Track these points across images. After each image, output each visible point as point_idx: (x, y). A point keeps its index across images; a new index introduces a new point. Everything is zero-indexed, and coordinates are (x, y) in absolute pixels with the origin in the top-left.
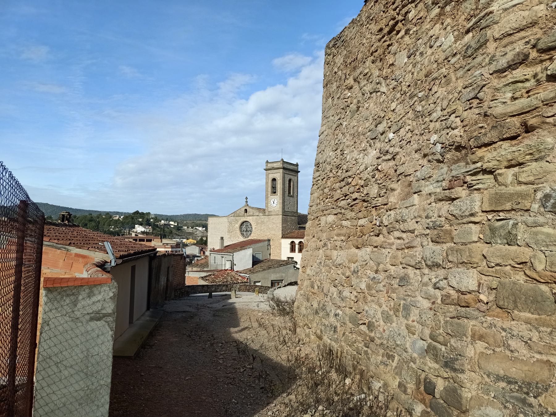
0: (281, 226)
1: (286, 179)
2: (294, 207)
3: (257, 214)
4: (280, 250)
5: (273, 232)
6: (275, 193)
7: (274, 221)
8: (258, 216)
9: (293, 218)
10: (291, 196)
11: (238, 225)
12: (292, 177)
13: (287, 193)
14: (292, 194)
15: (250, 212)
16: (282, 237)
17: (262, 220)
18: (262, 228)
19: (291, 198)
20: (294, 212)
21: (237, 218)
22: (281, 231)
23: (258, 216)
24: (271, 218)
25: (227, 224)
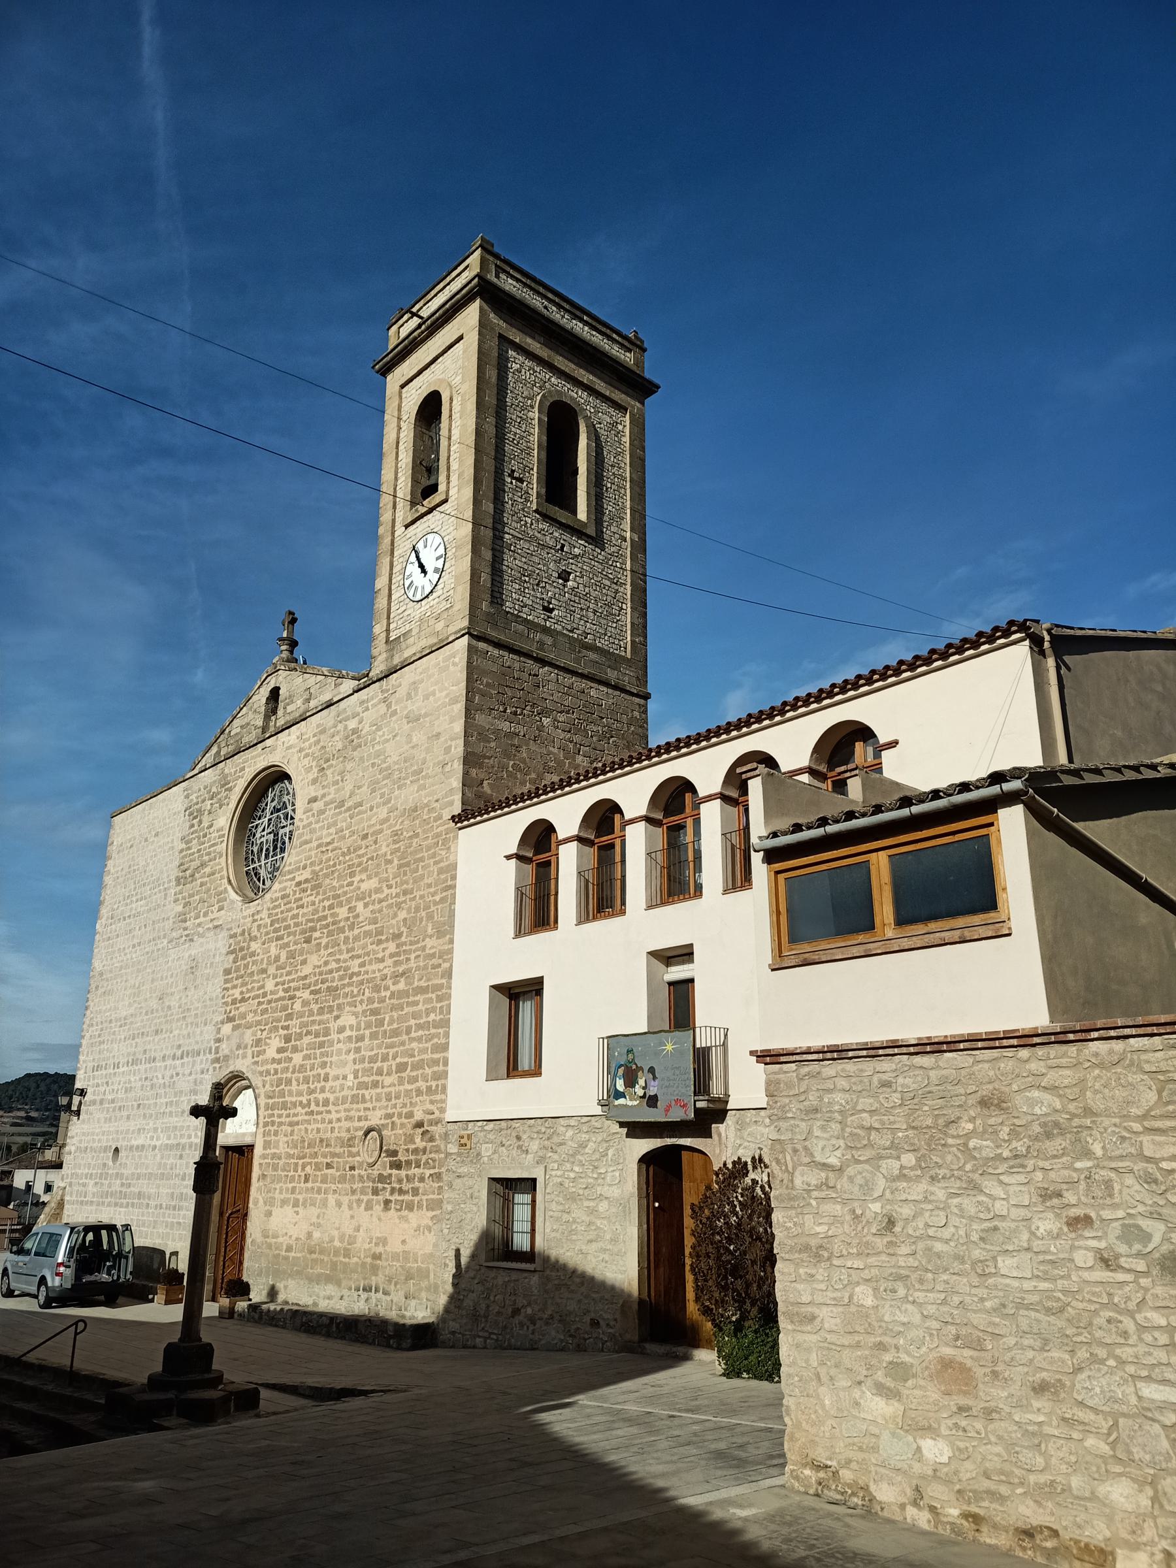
0: (459, 726)
1: (517, 391)
2: (610, 612)
3: (326, 697)
4: (446, 930)
5: (408, 796)
6: (432, 489)
7: (416, 705)
8: (329, 705)
9: (596, 692)
10: (577, 531)
11: (224, 820)
12: (579, 396)
13: (534, 486)
14: (582, 515)
15: (291, 699)
16: (464, 817)
17: (352, 724)
18: (349, 787)
19: (579, 547)
20: (616, 661)
21: (229, 767)
22: (458, 767)
23: (329, 705)
24: (402, 692)
25: (179, 825)
